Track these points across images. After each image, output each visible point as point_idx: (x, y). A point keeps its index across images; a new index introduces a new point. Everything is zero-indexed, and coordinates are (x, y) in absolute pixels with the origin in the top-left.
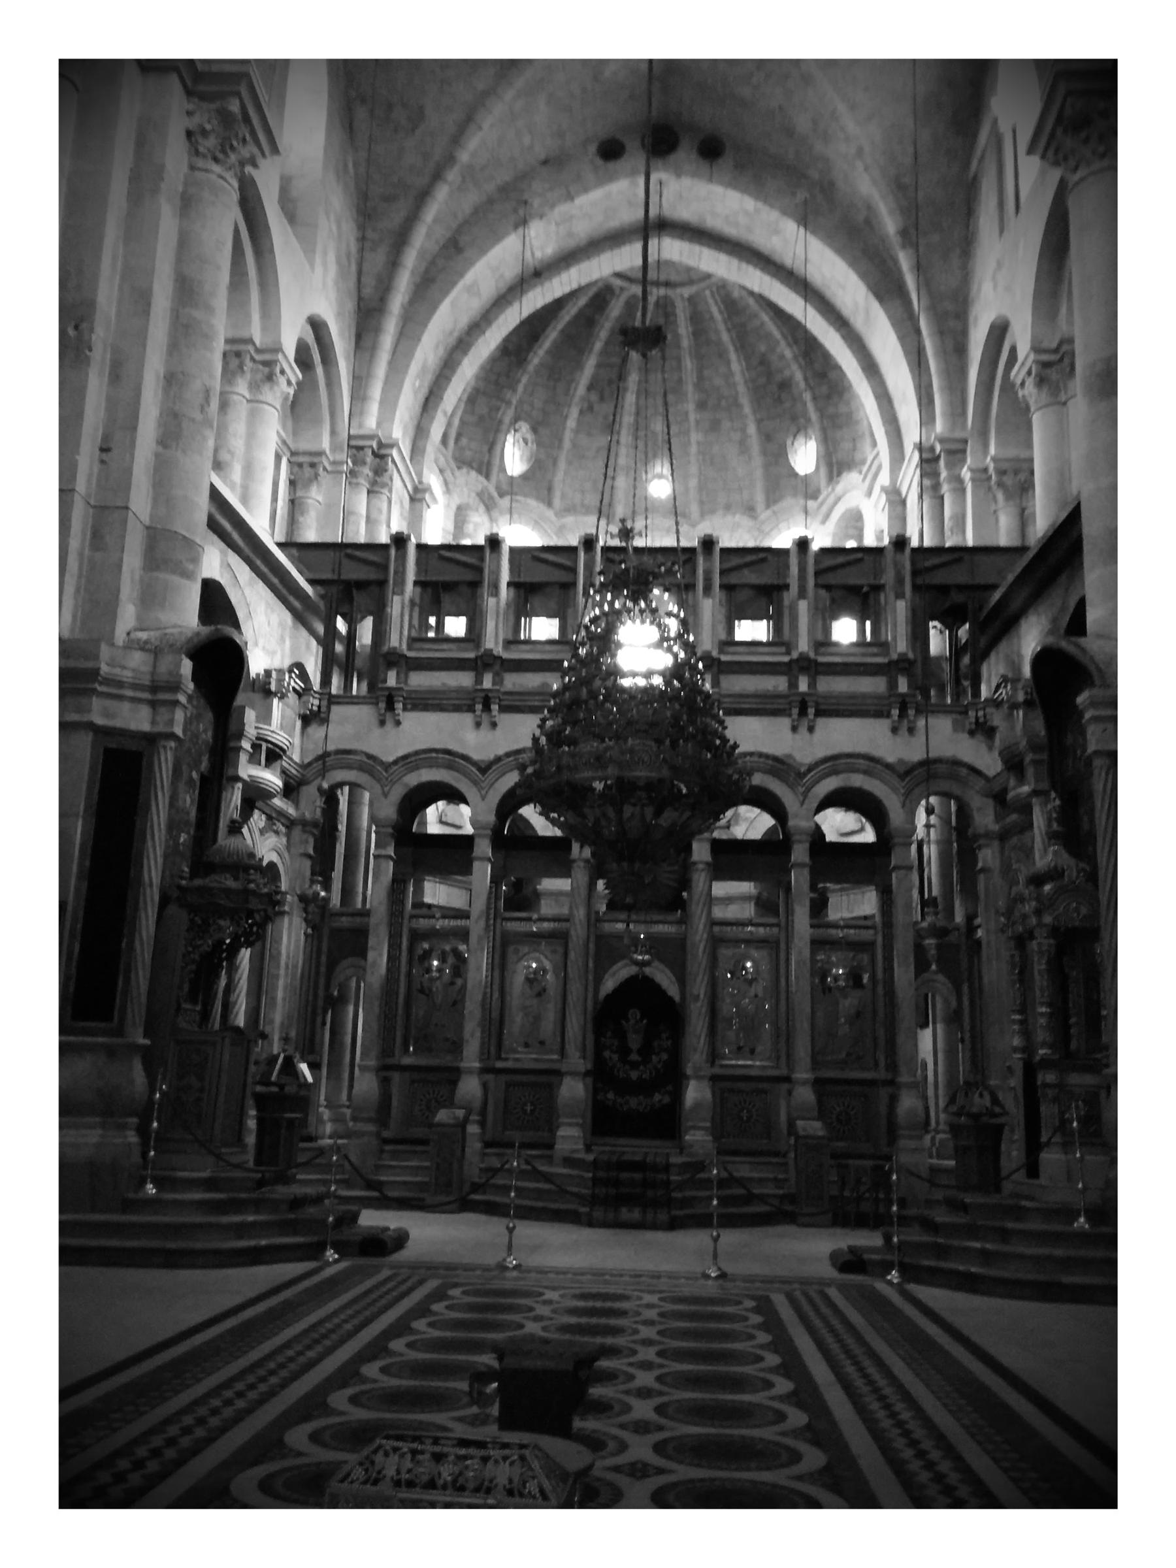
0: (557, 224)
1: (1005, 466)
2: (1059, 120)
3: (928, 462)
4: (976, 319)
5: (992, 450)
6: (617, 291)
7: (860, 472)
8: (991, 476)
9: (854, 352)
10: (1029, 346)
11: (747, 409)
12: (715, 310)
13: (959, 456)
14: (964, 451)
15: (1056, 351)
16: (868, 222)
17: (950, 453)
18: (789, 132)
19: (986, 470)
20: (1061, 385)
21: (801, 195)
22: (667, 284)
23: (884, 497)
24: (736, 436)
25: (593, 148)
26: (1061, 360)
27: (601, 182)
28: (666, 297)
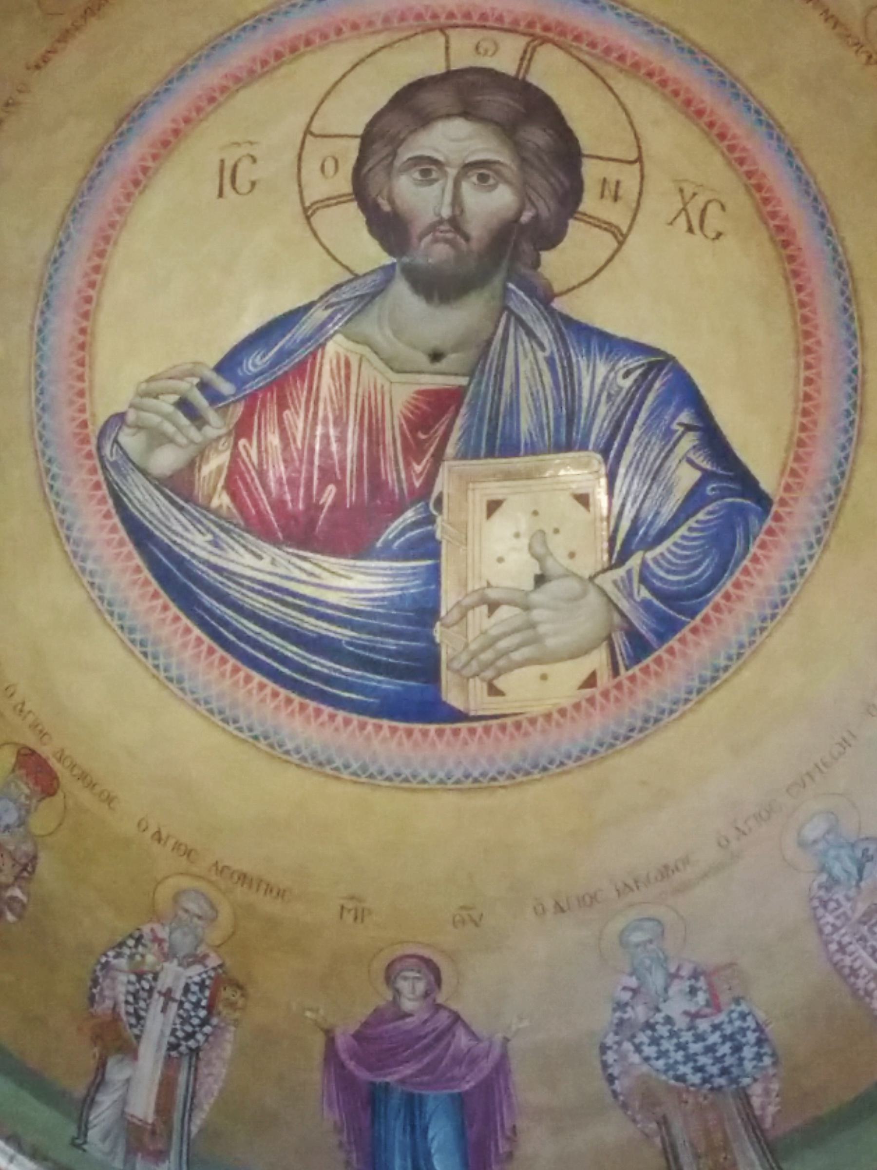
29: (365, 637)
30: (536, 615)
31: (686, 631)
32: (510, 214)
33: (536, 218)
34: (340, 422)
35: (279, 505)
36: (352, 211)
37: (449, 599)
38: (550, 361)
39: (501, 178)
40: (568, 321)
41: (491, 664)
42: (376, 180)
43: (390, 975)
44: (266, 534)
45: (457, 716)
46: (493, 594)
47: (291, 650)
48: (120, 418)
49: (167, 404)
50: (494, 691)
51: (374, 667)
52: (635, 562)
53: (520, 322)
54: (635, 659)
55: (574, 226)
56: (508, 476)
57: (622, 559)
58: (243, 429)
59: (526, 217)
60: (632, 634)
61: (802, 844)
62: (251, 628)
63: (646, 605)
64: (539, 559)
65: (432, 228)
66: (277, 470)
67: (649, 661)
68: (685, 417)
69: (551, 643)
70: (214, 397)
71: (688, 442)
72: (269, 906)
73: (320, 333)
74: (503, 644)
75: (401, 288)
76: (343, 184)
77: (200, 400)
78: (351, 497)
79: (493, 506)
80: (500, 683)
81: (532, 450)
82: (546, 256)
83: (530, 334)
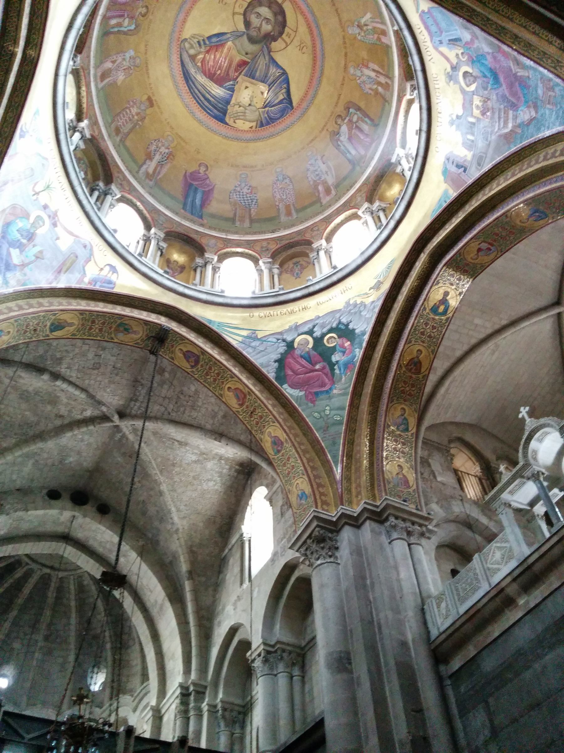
0: (14, 521)
1: (227, 706)
2: (310, 537)
3: (185, 695)
4: (219, 623)
5: (220, 695)
6: (23, 565)
7: (132, 696)
8: (218, 711)
9: (148, 626)
10: (261, 641)
11: (72, 646)
12: (72, 587)
13: (202, 695)
14: (204, 693)
15: (273, 646)
16: (171, 563)
17: (197, 692)
18: (144, 513)
19: (215, 706)
20: (275, 665)
21: (141, 543)
22: (52, 568)
23: (150, 714)
24: (60, 660)
25: (45, 491)
26: (276, 652)
27: (44, 508)
28: (49, 575)
29: (216, 102)
34: (225, 59)
35: (209, 70)
36: (242, 17)
37: (233, 101)
39: (271, 24)
42: (248, 14)
43: (200, 165)
44: (205, 75)
45: (227, 124)
47: (202, 99)
48: (186, 39)
49: (196, 40)
50: (235, 122)
52: (267, 109)
54: (260, 127)
55: (280, 40)
56: (252, 83)
57: (265, 107)
58: (208, 52)
60: (261, 122)
61: (276, 172)
62: (196, 91)
65: (255, 28)
66: (211, 63)
68: (285, 86)
70: (205, 44)
71: (284, 90)
72: (183, 144)
73: (227, 40)
75: (245, 37)
76: (242, 11)
77: (202, 43)
79: (247, 87)
81: (257, 80)
82: (273, 43)
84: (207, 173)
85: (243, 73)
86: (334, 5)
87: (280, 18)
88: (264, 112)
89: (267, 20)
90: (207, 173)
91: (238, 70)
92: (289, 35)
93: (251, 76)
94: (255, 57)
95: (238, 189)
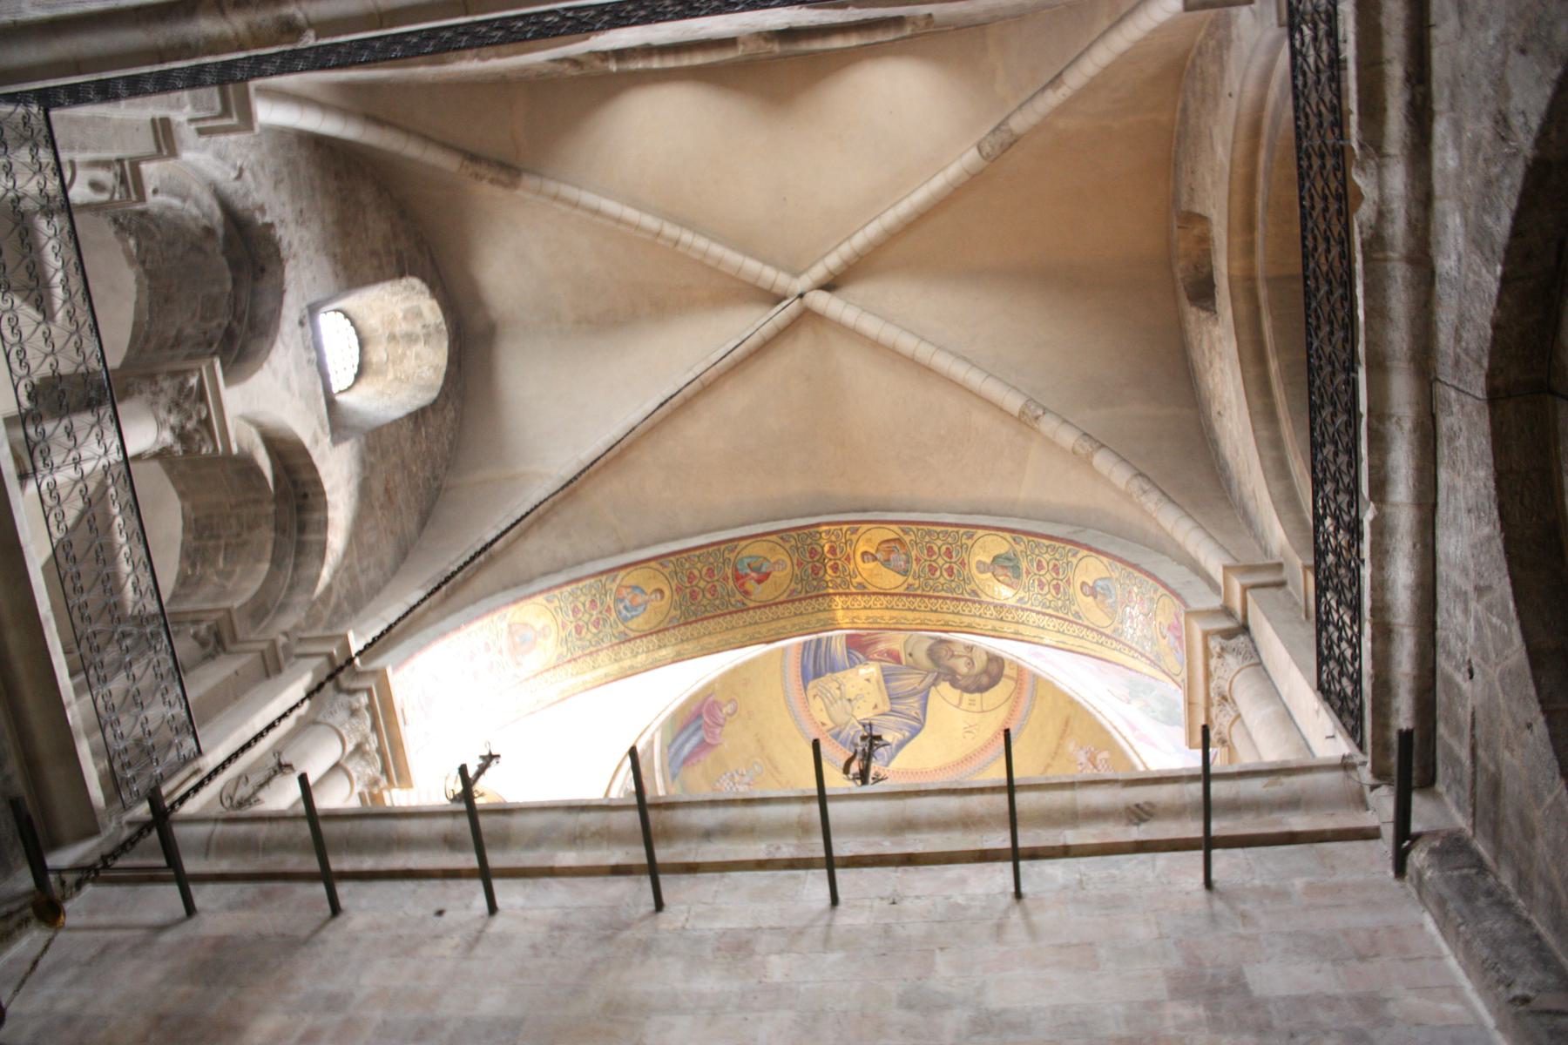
30: (839, 702)
31: (844, 749)
32: (959, 671)
33: (958, 680)
37: (838, 675)
38: (915, 688)
40: (928, 693)
41: (821, 692)
45: (805, 688)
46: (842, 687)
50: (815, 696)
51: (815, 662)
53: (925, 678)
55: (958, 692)
59: (958, 676)
60: (840, 733)
63: (849, 734)
64: (856, 699)
65: (950, 649)
67: (834, 741)
69: (832, 709)
74: (829, 695)
78: (864, 639)
80: (818, 698)
83: (922, 681)
84: (728, 718)
85: (883, 664)
86: (1053, 758)
87: (985, 680)
88: (854, 726)
89: (971, 663)
90: (728, 718)
91: (882, 655)
92: (972, 702)
93: (887, 677)
94: (915, 667)
95: (737, 778)
